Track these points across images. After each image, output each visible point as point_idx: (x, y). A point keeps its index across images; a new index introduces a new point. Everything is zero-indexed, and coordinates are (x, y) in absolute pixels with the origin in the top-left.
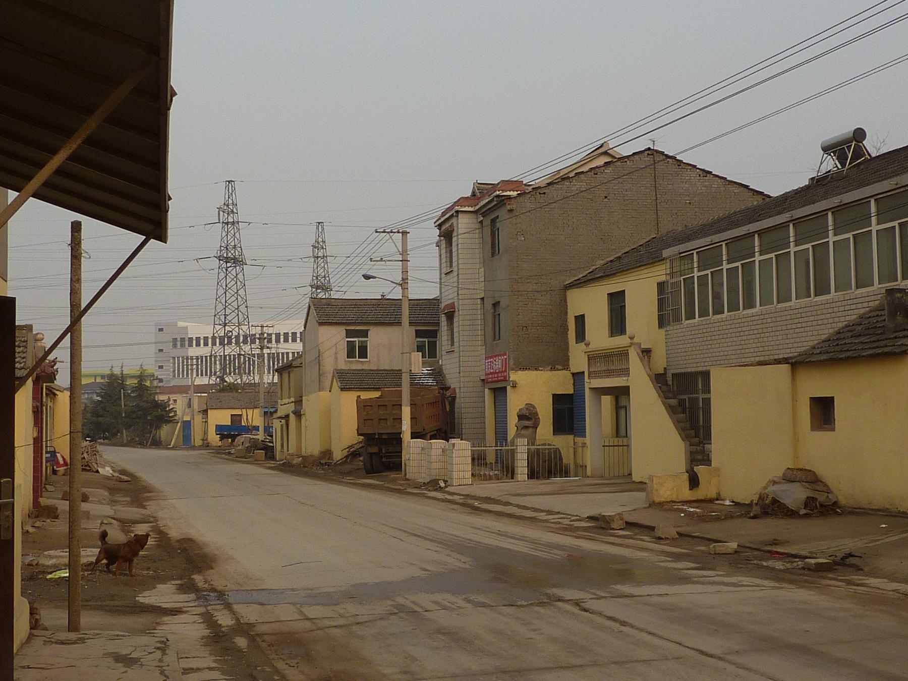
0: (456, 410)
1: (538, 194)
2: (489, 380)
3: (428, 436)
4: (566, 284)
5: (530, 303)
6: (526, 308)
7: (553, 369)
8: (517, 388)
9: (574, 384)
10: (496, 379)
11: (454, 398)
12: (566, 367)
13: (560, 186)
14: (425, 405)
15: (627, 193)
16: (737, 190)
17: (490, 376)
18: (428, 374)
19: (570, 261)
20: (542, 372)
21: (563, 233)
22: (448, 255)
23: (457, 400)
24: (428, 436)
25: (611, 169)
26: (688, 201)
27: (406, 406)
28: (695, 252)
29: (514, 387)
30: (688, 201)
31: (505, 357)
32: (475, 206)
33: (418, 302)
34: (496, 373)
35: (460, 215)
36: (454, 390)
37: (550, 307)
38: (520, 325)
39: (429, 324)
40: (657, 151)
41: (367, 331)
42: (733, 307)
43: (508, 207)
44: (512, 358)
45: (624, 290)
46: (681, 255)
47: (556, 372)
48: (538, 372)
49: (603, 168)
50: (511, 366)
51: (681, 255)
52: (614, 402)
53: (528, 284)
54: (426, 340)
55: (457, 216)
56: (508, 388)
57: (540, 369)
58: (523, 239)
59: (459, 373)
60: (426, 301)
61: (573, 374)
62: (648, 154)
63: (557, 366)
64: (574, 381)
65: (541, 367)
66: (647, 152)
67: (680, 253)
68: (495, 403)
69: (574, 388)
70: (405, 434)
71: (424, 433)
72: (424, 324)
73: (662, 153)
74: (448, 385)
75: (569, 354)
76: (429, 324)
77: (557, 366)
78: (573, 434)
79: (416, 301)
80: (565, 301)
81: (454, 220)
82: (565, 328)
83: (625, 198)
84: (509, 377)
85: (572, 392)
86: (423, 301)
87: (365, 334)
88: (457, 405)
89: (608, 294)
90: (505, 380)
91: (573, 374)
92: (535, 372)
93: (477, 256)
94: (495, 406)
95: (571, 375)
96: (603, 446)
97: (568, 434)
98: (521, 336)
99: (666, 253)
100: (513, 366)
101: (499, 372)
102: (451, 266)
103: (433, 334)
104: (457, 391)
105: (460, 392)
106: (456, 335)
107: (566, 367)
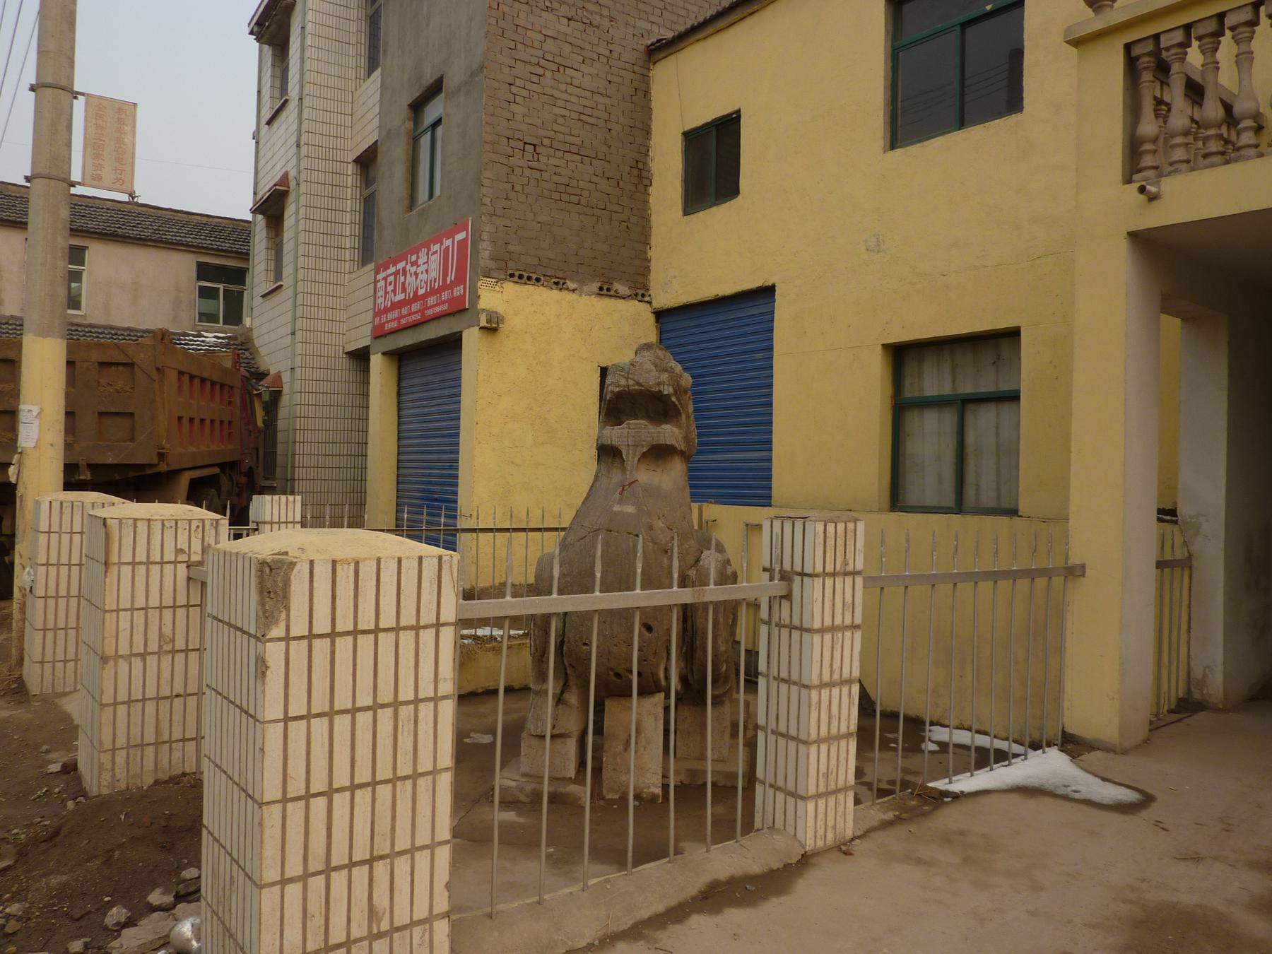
0: (281, 424)
2: (388, 327)
3: (184, 481)
5: (549, 74)
6: (538, 89)
7: (605, 291)
10: (417, 317)
11: (276, 396)
12: (640, 292)
14: (172, 376)
17: (393, 315)
20: (574, 296)
22: (278, 83)
23: (285, 400)
24: (184, 481)
27: (44, 333)
29: (492, 328)
31: (460, 236)
33: (211, 220)
34: (416, 298)
36: (278, 377)
37: (605, 100)
38: (518, 135)
39: (228, 253)
41: (84, 249)
44: (485, 236)
47: (613, 300)
48: (565, 293)
50: (482, 263)
52: (889, 391)
53: (544, 14)
54: (221, 287)
56: (471, 338)
57: (571, 285)
59: (293, 334)
60: (227, 221)
61: (660, 315)
65: (572, 280)
68: (399, 395)
70: (29, 462)
71: (163, 468)
72: (218, 252)
74: (262, 369)
75: (651, 254)
76: (228, 253)
77: (616, 286)
79: (205, 218)
80: (646, 94)
82: (641, 176)
84: (475, 297)
86: (220, 220)
88: (282, 413)
90: (459, 310)
91: (660, 315)
92: (555, 292)
93: (352, 62)
94: (399, 403)
95: (652, 318)
98: (517, 170)
100: (492, 265)
101: (432, 292)
102: (278, 275)
103: (238, 276)
104: (286, 378)
105: (293, 379)
106: (287, 259)
107: (640, 292)
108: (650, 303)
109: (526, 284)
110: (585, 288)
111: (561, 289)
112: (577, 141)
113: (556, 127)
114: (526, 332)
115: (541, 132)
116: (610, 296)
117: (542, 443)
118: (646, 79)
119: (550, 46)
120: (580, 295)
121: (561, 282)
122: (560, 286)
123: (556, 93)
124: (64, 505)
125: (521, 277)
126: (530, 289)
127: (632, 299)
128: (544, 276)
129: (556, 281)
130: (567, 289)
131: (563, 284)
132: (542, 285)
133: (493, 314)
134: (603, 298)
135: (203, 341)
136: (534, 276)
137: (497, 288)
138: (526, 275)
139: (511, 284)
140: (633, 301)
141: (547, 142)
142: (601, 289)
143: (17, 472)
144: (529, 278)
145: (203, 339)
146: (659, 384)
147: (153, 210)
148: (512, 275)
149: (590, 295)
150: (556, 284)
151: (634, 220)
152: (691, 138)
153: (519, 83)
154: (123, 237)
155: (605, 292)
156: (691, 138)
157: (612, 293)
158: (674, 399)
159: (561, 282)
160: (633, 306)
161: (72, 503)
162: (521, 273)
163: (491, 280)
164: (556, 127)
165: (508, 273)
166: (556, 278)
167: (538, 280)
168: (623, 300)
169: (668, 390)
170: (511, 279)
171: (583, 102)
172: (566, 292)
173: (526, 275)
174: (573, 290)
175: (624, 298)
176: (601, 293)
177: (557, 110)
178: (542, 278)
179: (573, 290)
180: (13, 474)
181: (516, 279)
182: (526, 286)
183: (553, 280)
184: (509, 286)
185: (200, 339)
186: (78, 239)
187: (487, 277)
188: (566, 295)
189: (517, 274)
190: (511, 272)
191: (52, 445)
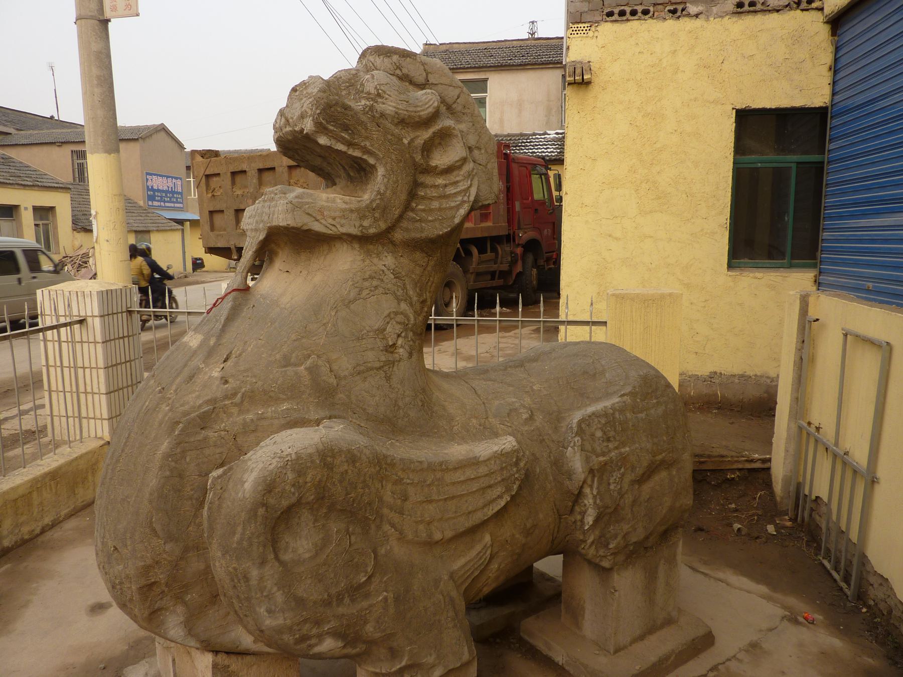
8: (595, 88)
9: (835, 69)
18: (554, 140)
20: (698, 22)
27: (92, 153)
41: (486, 80)
47: (759, 18)
57: (693, 9)
64: (837, 49)
69: (834, 83)
78: (814, 266)
87: (481, 85)
92: (671, 24)
95: (824, 31)
97: (791, 266)
108: (821, 9)
109: (628, 20)
110: (715, 9)
111: (678, 18)
114: (628, 80)
116: (755, 12)
117: (651, 212)
120: (707, 19)
121: (680, 7)
122: (679, 14)
124: (58, 292)
125: (622, 13)
126: (635, 25)
127: (791, 9)
128: (655, 5)
129: (672, 8)
130: (689, 15)
131: (683, 10)
132: (652, 17)
133: (578, 66)
134: (743, 17)
135: (544, 138)
136: (640, 9)
137: (591, 33)
138: (628, 10)
139: (609, 25)
140: (792, 12)
142: (740, 5)
143: (94, 262)
144: (634, 13)
145: (546, 136)
146: (302, 116)
147: (545, 41)
148: (610, 14)
149: (722, 17)
150: (674, 12)
154: (509, 65)
155: (746, 8)
157: (759, 7)
158: (323, 140)
159: (680, 7)
160: (796, 17)
161: (56, 291)
162: (622, 8)
163: (582, 25)
165: (605, 13)
166: (672, 4)
167: (646, 12)
168: (775, 15)
169: (308, 126)
170: (608, 19)
172: (686, 19)
173: (628, 10)
174: (697, 16)
175: (778, 11)
176: (739, 10)
178: (651, 9)
179: (697, 16)
180: (93, 264)
181: (616, 17)
182: (629, 24)
183: (668, 8)
184: (608, 29)
185: (543, 137)
186: (482, 73)
187: (578, 23)
188: (686, 24)
189: (616, 11)
190: (609, 10)
191: (108, 241)
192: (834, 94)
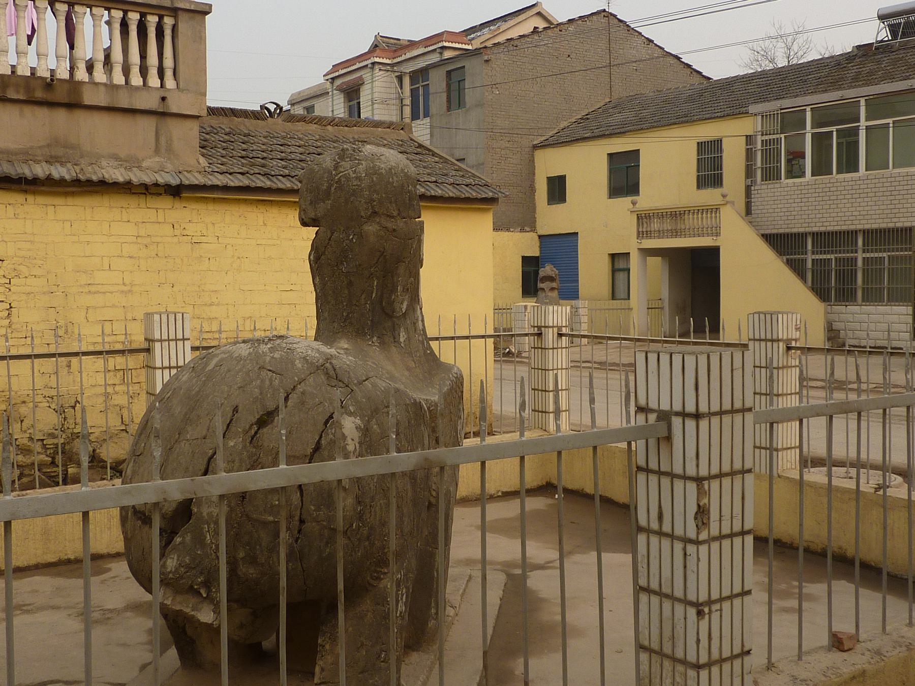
1: (511, 46)
4: (534, 143)
6: (499, 167)
7: (522, 230)
12: (533, 229)
13: (531, 40)
15: (586, 53)
16: (672, 61)
19: (538, 119)
21: (532, 90)
25: (573, 27)
26: (635, 68)
28: (808, 109)
30: (635, 68)
32: (394, 58)
35: (377, 67)
37: (520, 166)
40: (612, 14)
42: (821, 168)
43: (486, 58)
45: (639, 150)
46: (782, 111)
49: (567, 26)
51: (782, 111)
52: (611, 265)
55: (372, 68)
57: (512, 230)
58: (498, 93)
61: (540, 237)
62: (604, 16)
63: (526, 228)
66: (603, 14)
67: (781, 109)
73: (615, 16)
75: (536, 216)
77: (526, 228)
80: (533, 161)
81: (366, 75)
82: (532, 189)
83: (585, 58)
85: (537, 254)
89: (608, 154)
91: (540, 237)
95: (538, 237)
96: (648, 308)
99: (753, 109)
107: (533, 229)
112: (512, 182)
113: (506, 179)
115: (502, 181)
118: (533, 156)
119: (503, 152)
123: (505, 168)
141: (503, 184)
151: (530, 205)
152: (550, 180)
153: (495, 167)
156: (550, 180)
164: (506, 179)
169: (554, 276)
171: (514, 168)
177: (506, 173)
192: (541, 253)
